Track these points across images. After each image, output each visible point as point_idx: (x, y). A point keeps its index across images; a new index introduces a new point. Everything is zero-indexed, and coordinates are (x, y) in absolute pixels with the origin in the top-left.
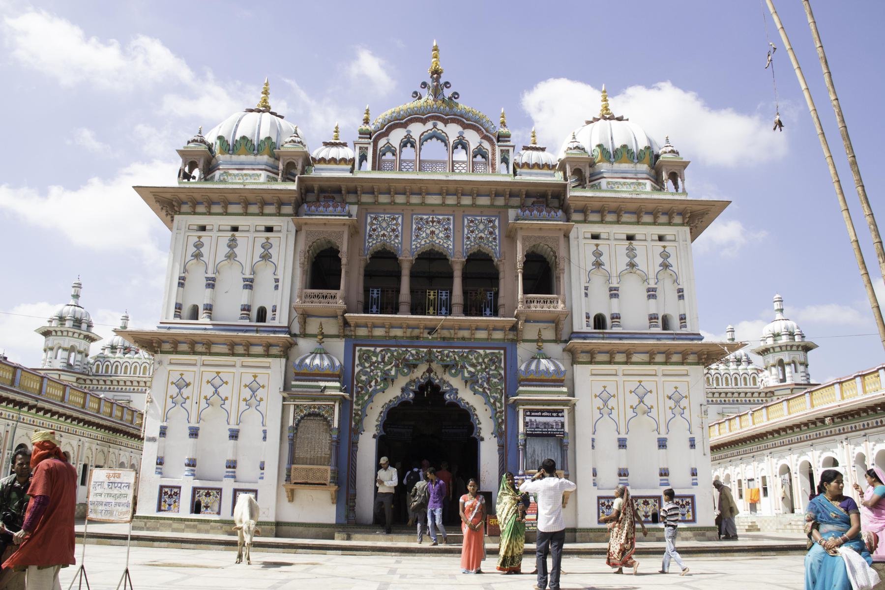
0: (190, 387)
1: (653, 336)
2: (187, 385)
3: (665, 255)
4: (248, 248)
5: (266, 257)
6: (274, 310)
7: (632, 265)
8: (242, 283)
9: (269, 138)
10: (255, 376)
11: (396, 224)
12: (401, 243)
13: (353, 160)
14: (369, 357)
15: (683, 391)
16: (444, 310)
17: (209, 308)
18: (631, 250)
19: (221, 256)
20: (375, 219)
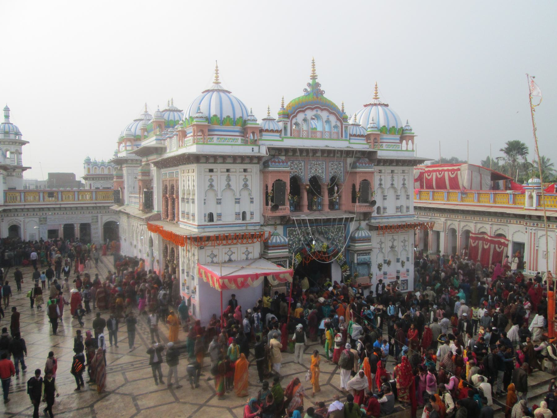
0: (217, 257)
1: (399, 217)
2: (215, 256)
3: (404, 180)
4: (237, 181)
5: (246, 186)
6: (252, 214)
7: (392, 184)
8: (234, 201)
9: (241, 117)
10: (247, 248)
11: (301, 166)
12: (304, 176)
13: (281, 131)
14: (293, 233)
15: (406, 239)
16: (320, 208)
17: (219, 215)
18: (392, 177)
19: (224, 187)
20: (292, 163)
